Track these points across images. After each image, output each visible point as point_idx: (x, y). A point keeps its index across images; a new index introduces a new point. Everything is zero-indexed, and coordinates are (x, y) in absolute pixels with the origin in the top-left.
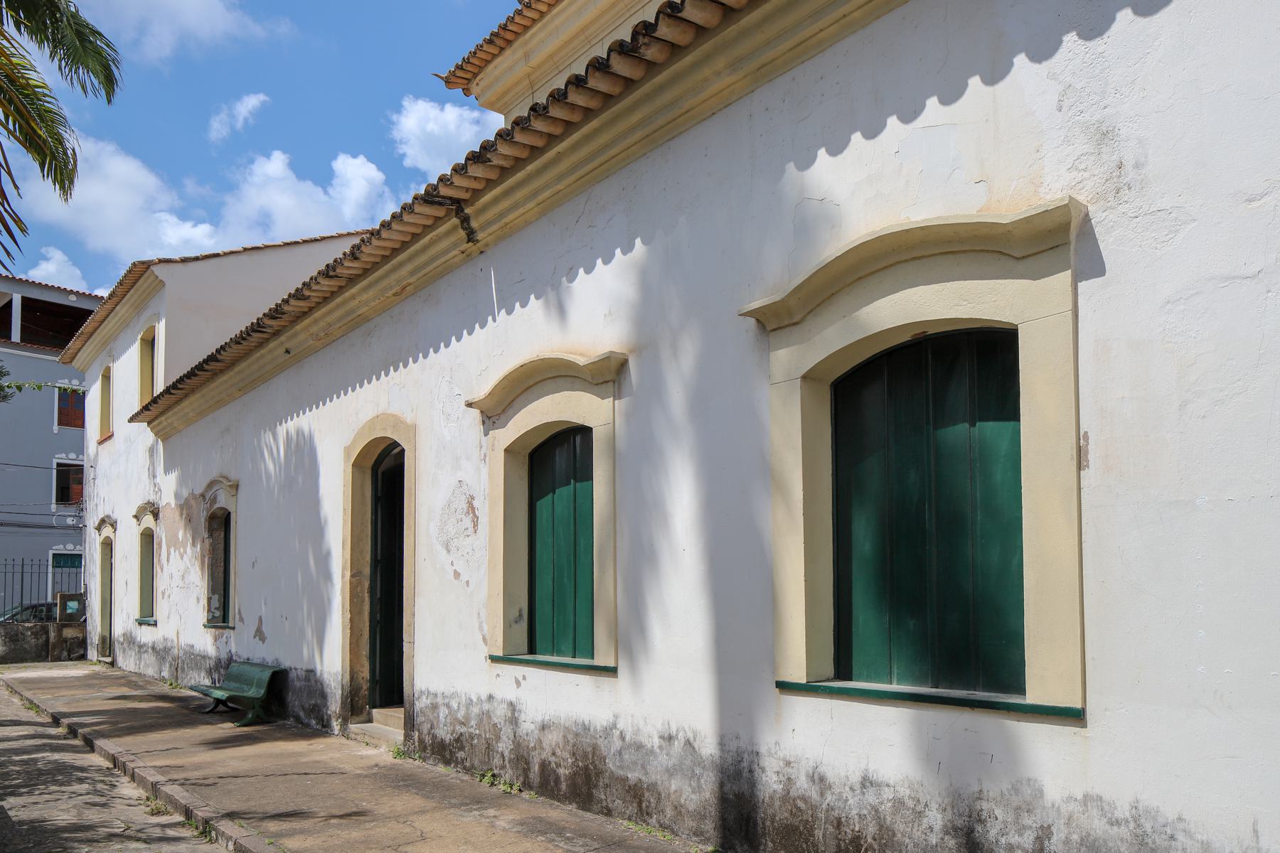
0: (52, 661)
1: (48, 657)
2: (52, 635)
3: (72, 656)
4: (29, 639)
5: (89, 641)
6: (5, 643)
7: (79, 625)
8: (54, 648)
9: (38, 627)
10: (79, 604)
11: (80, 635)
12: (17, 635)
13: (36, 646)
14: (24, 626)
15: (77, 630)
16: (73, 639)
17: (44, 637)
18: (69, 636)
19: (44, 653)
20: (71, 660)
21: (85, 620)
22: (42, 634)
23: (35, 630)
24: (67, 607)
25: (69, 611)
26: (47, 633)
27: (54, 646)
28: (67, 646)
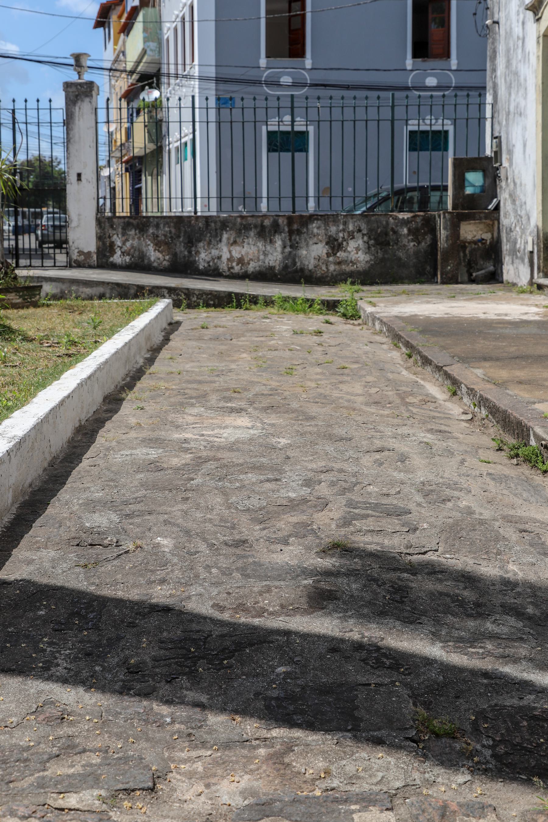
0: (443, 283)
1: (435, 275)
2: (443, 234)
3: (474, 274)
4: (405, 241)
5: (506, 247)
6: (369, 248)
7: (486, 218)
8: (445, 260)
9: (418, 220)
10: (485, 176)
11: (487, 236)
12: (386, 234)
13: (416, 253)
14: (396, 218)
15: (482, 226)
16: (475, 243)
17: (428, 238)
18: (469, 237)
19: (428, 268)
20: (472, 281)
21: (497, 208)
22: (425, 234)
23: (413, 225)
24: (466, 184)
25: (469, 191)
26: (433, 230)
27: (447, 255)
28: (465, 255)
